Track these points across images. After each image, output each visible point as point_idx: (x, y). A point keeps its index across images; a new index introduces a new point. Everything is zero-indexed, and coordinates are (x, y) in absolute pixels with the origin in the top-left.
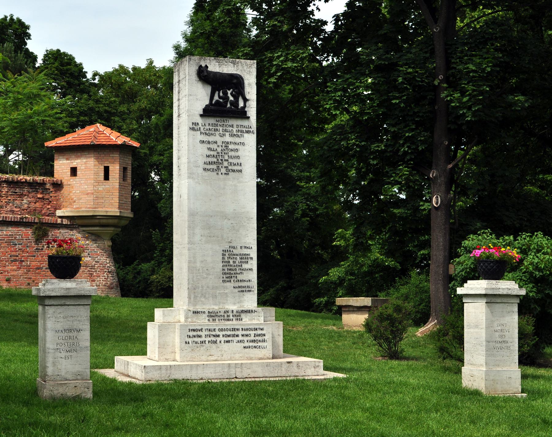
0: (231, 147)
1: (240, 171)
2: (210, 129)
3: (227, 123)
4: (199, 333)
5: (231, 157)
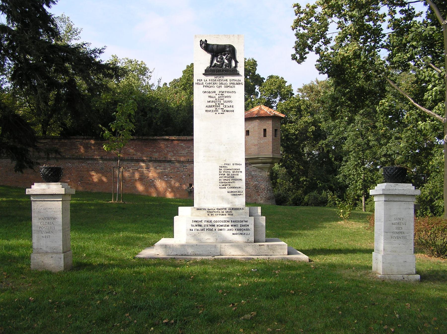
0: (226, 94)
1: (233, 111)
2: (210, 83)
3: (223, 79)
4: (200, 223)
5: (226, 102)
